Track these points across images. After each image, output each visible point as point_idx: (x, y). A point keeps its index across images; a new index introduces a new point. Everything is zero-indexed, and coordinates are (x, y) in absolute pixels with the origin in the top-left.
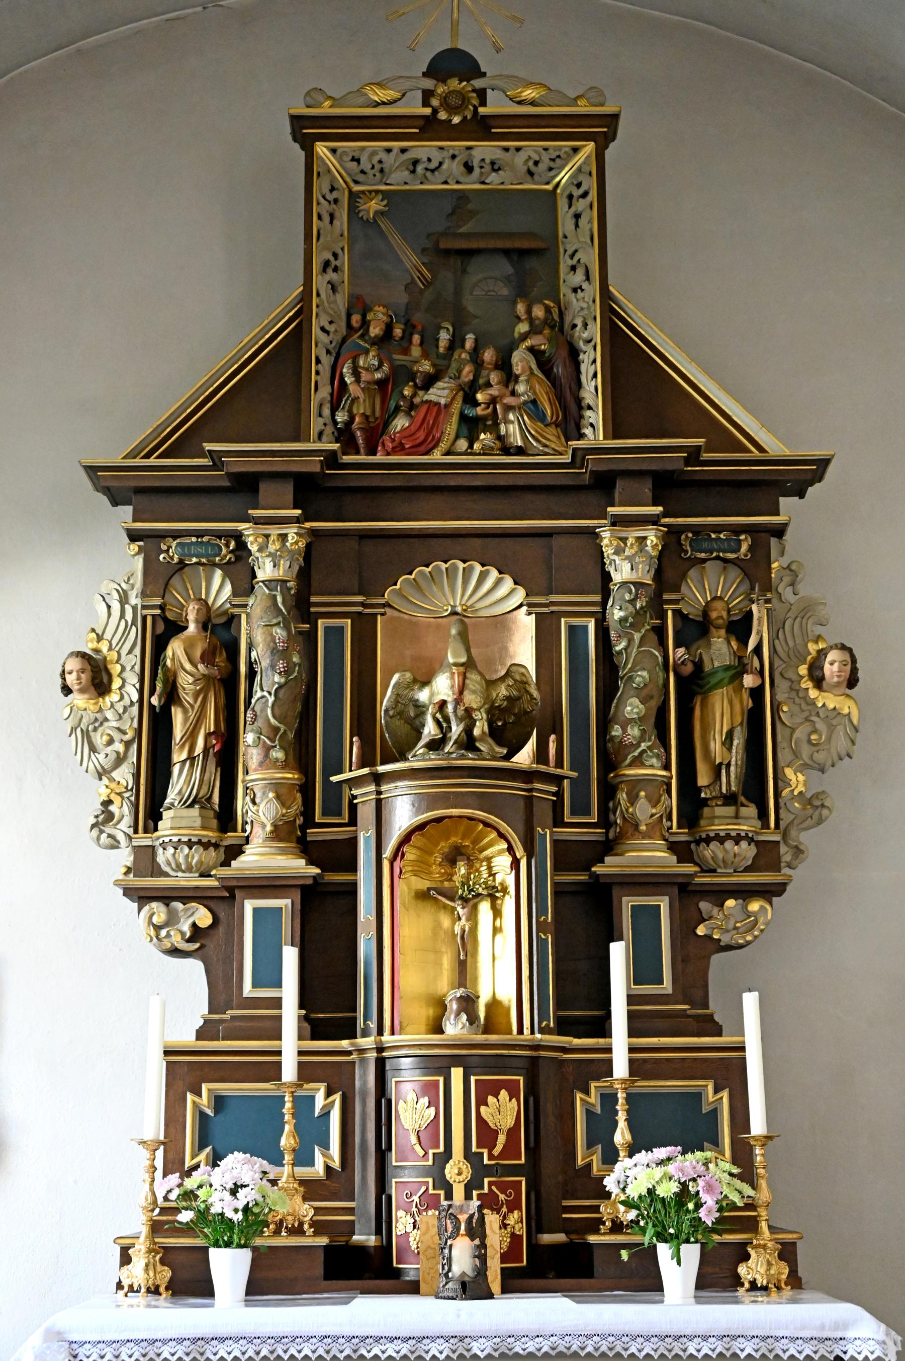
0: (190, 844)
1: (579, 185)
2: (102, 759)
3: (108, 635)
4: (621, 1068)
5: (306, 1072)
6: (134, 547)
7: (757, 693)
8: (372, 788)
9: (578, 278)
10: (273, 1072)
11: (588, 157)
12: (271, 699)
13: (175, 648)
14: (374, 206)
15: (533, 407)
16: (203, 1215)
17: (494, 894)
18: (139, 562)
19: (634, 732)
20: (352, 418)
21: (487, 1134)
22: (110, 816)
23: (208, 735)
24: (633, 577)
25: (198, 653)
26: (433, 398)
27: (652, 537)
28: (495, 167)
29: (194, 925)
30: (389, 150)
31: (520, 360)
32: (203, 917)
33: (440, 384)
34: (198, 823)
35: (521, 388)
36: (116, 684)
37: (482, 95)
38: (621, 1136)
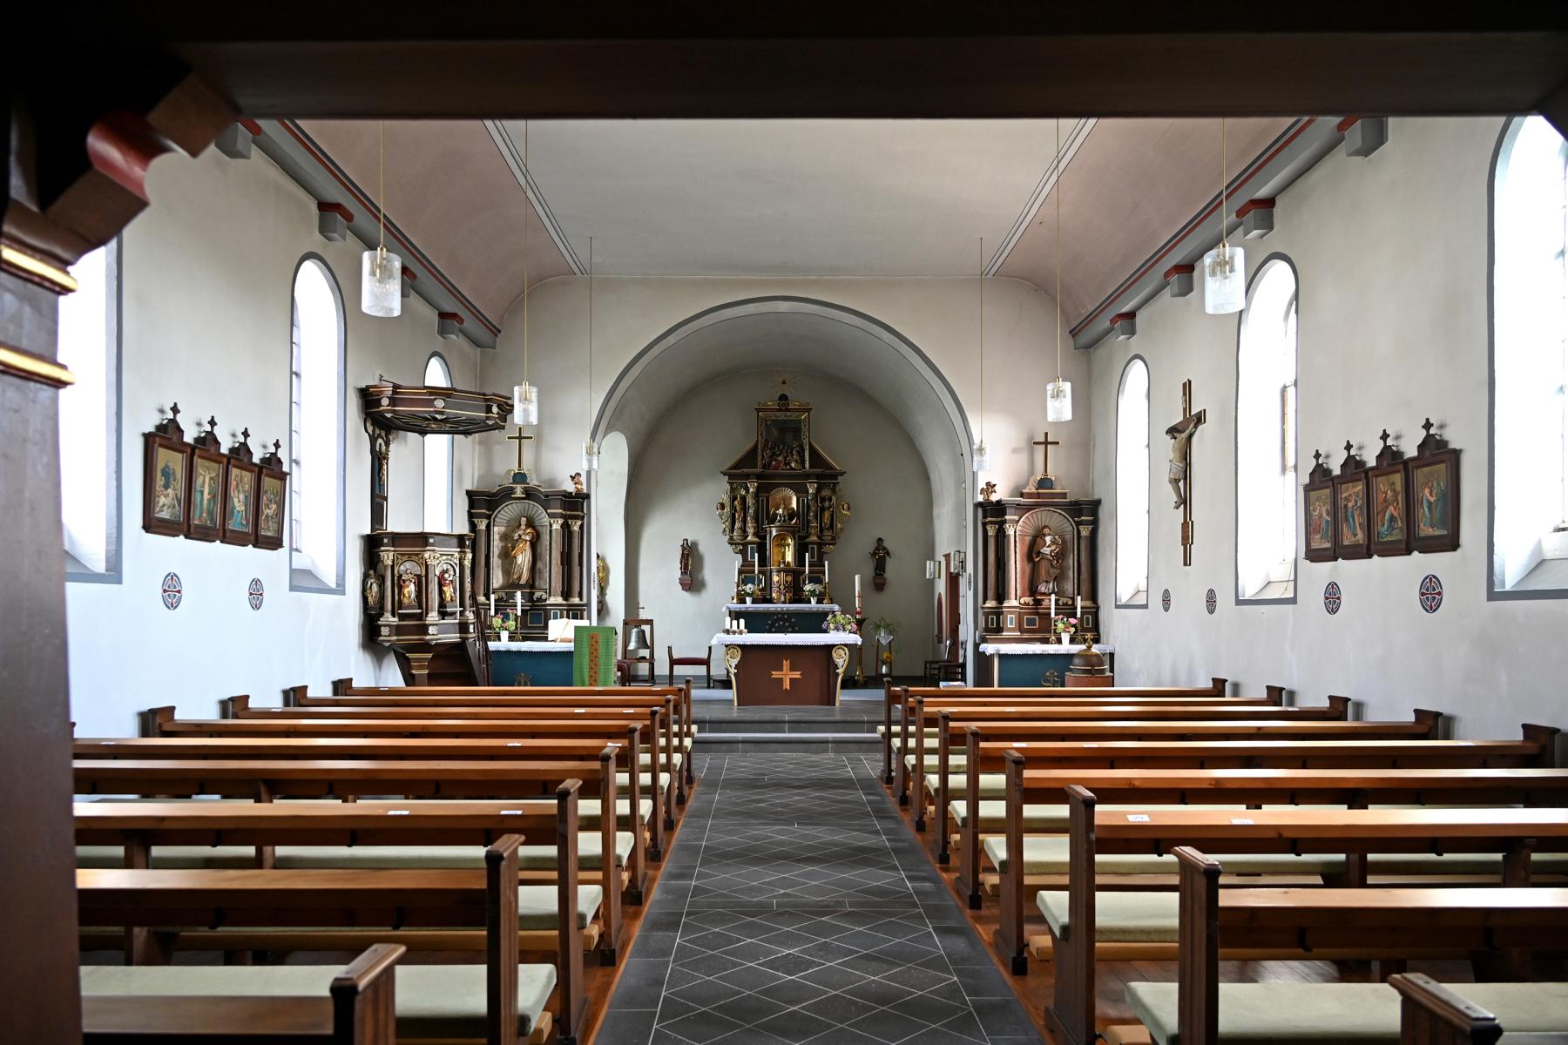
4: (807, 572)
5: (759, 572)
7: (833, 511)
13: (736, 502)
14: (769, 422)
15: (796, 461)
16: (745, 593)
17: (789, 545)
21: (787, 582)
27: (816, 486)
31: (794, 452)
32: (741, 547)
38: (807, 582)
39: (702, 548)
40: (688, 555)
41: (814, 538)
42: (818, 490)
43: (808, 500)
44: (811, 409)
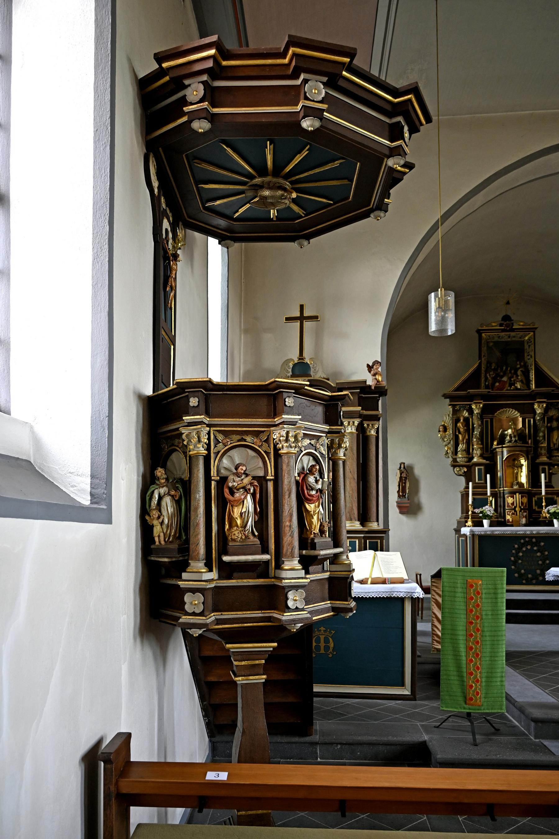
0: (465, 458)
1: (530, 340)
2: (445, 443)
3: (446, 422)
6: (450, 407)
8: (501, 449)
9: (529, 357)
10: (487, 494)
11: (532, 335)
12: (478, 433)
13: (460, 425)
14: (491, 344)
15: (521, 381)
18: (451, 409)
19: (541, 438)
20: (489, 383)
22: (448, 453)
23: (466, 439)
24: (541, 412)
25: (464, 425)
26: (504, 380)
27: (545, 405)
28: (514, 337)
29: (464, 471)
30: (495, 334)
31: (519, 372)
32: (466, 470)
33: (505, 377)
34: (465, 454)
35: (519, 378)
36: (448, 431)
37: (513, 324)
39: (417, 472)
40: (406, 478)
41: (544, 459)
42: (546, 410)
43: (534, 421)
44: (536, 328)
